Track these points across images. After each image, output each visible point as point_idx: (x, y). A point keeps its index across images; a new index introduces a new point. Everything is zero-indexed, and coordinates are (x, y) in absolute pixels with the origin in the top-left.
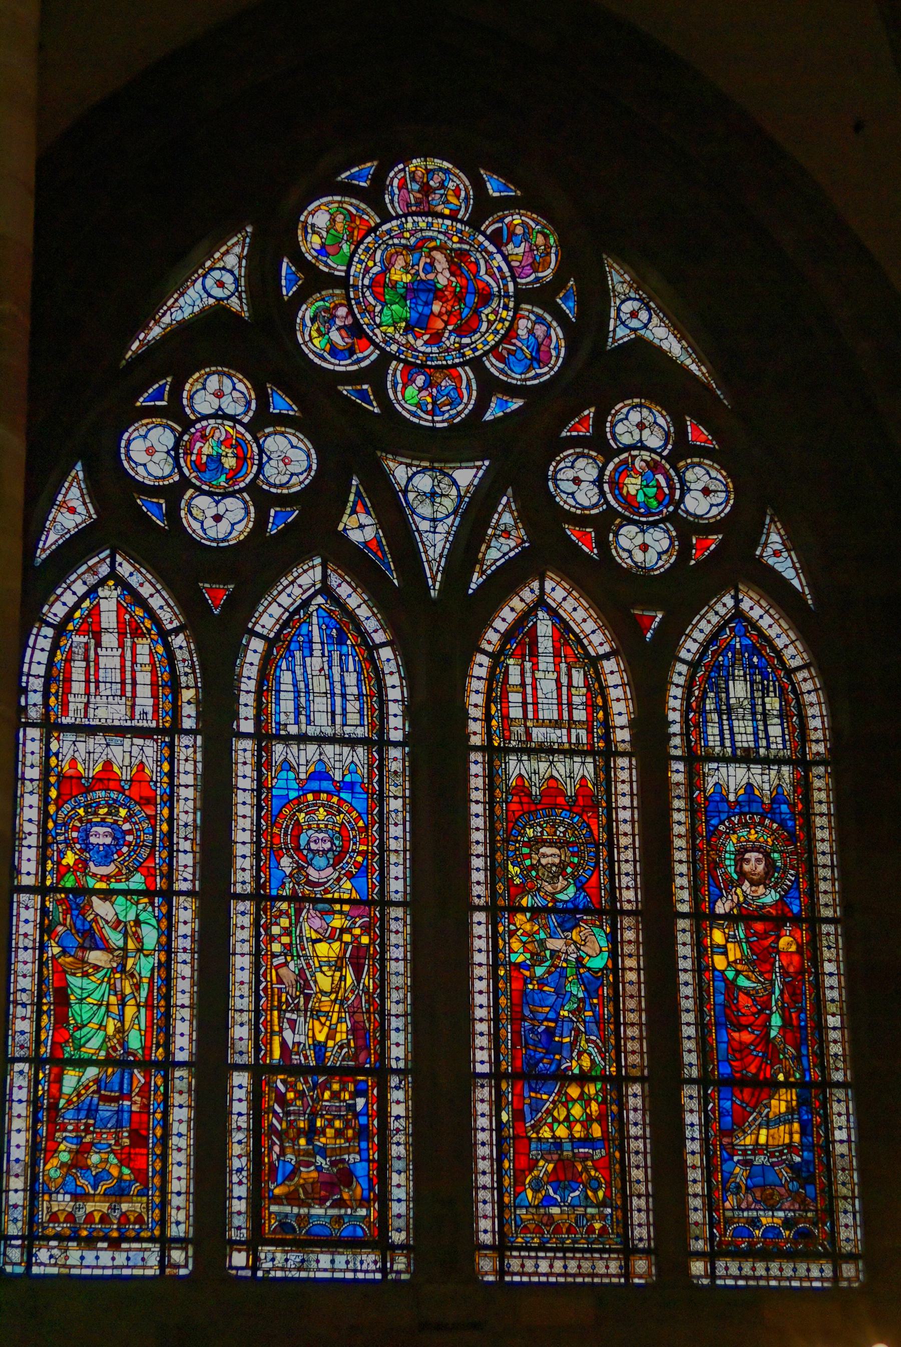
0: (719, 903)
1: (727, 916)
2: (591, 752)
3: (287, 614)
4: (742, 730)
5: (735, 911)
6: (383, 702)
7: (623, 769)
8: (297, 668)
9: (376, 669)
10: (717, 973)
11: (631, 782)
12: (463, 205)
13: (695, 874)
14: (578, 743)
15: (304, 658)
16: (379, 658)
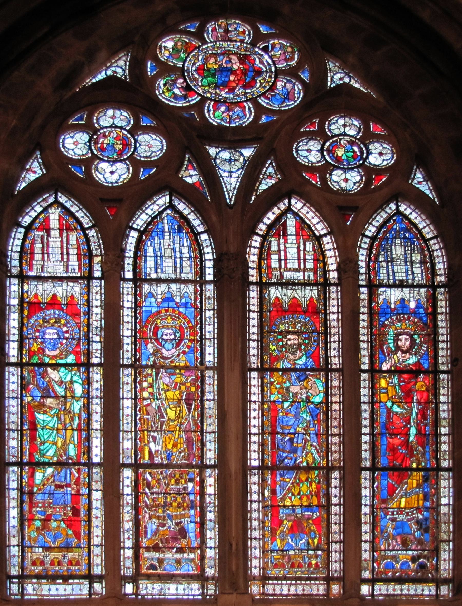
0: (384, 364)
1: (388, 371)
2: (316, 284)
3: (150, 218)
4: (399, 271)
5: (393, 369)
6: (202, 261)
7: (333, 292)
8: (156, 245)
9: (199, 245)
10: (381, 404)
11: (338, 299)
12: (247, 37)
13: (372, 349)
14: (308, 280)
15: (160, 240)
16: (201, 239)
